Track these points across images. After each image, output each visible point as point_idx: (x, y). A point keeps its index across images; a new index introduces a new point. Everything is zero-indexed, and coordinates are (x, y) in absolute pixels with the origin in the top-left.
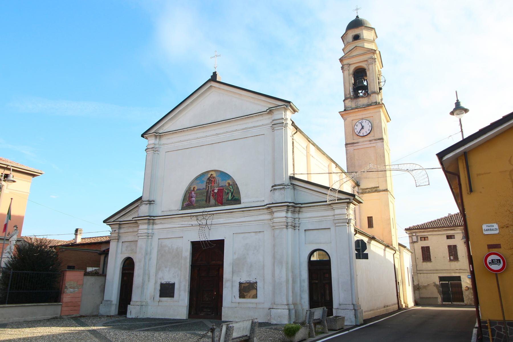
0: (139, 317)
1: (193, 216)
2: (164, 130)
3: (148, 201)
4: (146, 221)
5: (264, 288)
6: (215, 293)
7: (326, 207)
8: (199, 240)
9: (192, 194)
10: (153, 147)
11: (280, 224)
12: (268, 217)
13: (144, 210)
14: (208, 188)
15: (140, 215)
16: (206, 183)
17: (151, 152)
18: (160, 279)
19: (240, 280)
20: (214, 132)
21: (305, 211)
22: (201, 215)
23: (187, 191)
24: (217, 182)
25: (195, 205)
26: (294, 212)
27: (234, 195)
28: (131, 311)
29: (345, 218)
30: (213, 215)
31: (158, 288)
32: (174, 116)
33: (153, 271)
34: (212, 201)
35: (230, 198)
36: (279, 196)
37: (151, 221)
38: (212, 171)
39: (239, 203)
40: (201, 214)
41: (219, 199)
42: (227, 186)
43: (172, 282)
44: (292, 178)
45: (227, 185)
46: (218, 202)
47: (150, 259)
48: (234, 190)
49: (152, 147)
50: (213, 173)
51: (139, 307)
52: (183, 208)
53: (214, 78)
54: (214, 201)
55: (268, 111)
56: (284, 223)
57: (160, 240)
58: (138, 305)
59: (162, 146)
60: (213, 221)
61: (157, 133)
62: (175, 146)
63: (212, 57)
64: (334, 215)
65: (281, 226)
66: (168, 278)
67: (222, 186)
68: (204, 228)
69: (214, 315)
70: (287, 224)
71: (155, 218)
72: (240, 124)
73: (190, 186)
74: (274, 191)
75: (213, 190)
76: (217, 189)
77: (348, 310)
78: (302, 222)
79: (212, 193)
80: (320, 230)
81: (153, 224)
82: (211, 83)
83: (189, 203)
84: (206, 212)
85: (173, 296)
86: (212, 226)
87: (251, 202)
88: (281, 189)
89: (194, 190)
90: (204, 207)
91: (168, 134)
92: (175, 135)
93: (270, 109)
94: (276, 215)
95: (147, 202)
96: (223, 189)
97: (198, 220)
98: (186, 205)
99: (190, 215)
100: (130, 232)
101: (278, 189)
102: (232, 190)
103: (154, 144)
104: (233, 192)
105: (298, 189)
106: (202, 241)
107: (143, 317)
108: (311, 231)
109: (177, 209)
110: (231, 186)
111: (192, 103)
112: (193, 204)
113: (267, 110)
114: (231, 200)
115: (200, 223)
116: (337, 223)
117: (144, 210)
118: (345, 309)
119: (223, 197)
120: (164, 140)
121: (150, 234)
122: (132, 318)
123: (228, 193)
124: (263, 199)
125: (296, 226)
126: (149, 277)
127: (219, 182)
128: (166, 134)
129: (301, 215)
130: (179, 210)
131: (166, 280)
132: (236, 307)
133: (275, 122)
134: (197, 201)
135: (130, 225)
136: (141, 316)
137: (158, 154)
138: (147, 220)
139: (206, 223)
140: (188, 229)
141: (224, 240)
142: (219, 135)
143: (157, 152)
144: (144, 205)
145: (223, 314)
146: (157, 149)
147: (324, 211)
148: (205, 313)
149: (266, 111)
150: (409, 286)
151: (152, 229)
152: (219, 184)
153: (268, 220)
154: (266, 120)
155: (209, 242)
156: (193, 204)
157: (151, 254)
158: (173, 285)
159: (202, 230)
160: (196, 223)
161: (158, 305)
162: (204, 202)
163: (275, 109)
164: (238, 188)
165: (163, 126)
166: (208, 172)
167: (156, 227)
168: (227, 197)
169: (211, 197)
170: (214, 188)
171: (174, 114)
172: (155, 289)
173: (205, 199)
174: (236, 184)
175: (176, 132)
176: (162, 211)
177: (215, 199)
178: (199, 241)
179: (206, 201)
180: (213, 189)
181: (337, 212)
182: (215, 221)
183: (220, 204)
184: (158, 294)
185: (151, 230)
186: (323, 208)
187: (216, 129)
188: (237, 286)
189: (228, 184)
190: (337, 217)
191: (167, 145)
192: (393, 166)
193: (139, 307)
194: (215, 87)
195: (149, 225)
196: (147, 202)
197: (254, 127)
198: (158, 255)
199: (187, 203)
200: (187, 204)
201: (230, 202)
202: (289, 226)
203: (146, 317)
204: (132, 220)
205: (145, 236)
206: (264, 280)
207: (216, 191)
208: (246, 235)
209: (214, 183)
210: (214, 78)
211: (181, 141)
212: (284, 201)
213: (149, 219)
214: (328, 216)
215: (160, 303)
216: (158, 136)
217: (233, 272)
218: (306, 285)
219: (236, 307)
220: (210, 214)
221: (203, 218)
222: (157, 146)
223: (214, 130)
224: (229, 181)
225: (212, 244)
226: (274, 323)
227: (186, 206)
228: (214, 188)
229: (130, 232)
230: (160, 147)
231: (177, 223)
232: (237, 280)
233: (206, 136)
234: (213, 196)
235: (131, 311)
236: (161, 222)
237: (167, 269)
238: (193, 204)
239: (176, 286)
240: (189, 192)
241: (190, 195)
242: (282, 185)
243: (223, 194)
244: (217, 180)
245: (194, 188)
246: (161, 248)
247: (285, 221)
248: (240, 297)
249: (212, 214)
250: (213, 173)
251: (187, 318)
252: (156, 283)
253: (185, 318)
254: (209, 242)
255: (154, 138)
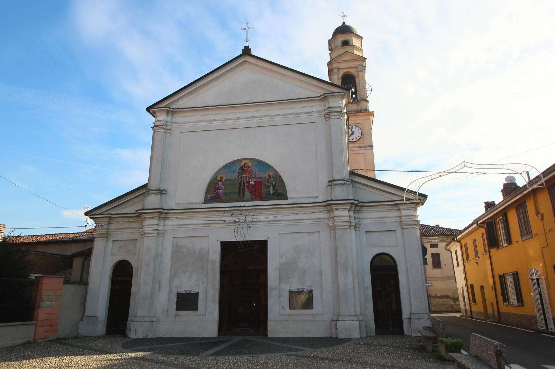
0: (149, 337)
1: (227, 211)
2: (179, 106)
3: (159, 190)
4: (157, 215)
5: (322, 297)
6: (255, 304)
7: (390, 207)
8: (236, 240)
9: (219, 184)
10: (165, 124)
11: (343, 223)
12: (324, 215)
13: (153, 201)
14: (240, 179)
15: (147, 207)
16: (239, 173)
17: (160, 131)
18: (177, 287)
19: (290, 288)
20: (289, 112)
21: (365, 211)
22: (237, 210)
23: (211, 181)
24: (254, 172)
25: (224, 198)
26: (354, 212)
27: (276, 189)
28: (136, 330)
29: (414, 220)
30: (255, 210)
31: (175, 299)
32: (194, 90)
33: (165, 277)
34: (248, 194)
35: (271, 192)
36: (339, 193)
37: (163, 215)
38: (246, 159)
39: (286, 198)
40: (238, 208)
41: (257, 193)
42: (267, 177)
43: (194, 290)
44: (352, 173)
45: (267, 177)
46: (255, 195)
47: (161, 263)
48: (276, 183)
49: (163, 124)
50: (247, 162)
51: (150, 323)
52: (206, 202)
53: (247, 51)
54: (250, 194)
55: (322, 97)
56: (348, 223)
57: (174, 239)
58: (148, 322)
59: (175, 125)
60: (254, 217)
61: (170, 108)
62: (194, 126)
63: (243, 29)
64: (400, 217)
65: (344, 226)
66: (187, 286)
67: (261, 178)
68: (241, 226)
69: (253, 330)
70: (350, 224)
71: (170, 211)
72: (283, 109)
73: (216, 175)
74: (334, 186)
75: (249, 182)
76: (254, 180)
77: (423, 320)
78: (363, 222)
79: (247, 186)
80: (383, 233)
81: (166, 218)
82: (245, 58)
83: (214, 195)
84: (244, 206)
85: (196, 309)
86: (253, 223)
87: (301, 198)
88: (342, 184)
89: (221, 180)
90: (238, 201)
91: (185, 110)
92: (194, 114)
93: (325, 95)
94: (336, 213)
95: (157, 192)
96: (262, 181)
97: (233, 216)
98: (210, 197)
99: (222, 209)
100: (126, 228)
101: (338, 184)
102: (274, 183)
103: (166, 122)
104: (276, 185)
105: (356, 186)
106: (238, 241)
107: (153, 337)
108: (373, 233)
109: (199, 201)
110: (273, 178)
111: (218, 77)
112: (221, 196)
113: (320, 95)
114: (274, 194)
115: (235, 219)
116: (404, 225)
117: (153, 201)
118: (420, 319)
119: (263, 191)
120: (178, 118)
121: (163, 231)
122: (138, 339)
123: (268, 186)
124: (316, 195)
125: (356, 226)
126: (160, 285)
127: (255, 173)
128: (182, 111)
129: (361, 215)
130: (202, 204)
131: (185, 289)
132: (286, 320)
133: (330, 110)
134: (226, 194)
135: (129, 219)
136: (151, 336)
137: (170, 134)
138: (159, 213)
139: (245, 220)
140: (216, 227)
141: (267, 240)
142: (256, 119)
143: (169, 131)
144: (153, 195)
145: (269, 329)
146: (169, 128)
147: (385, 211)
148: (241, 328)
149: (320, 97)
150: (493, 290)
151: (164, 225)
152: (256, 175)
153: (324, 219)
154: (317, 107)
155: (249, 242)
156: (221, 196)
157: (162, 257)
158: (196, 295)
159: (239, 228)
160: (230, 219)
161: (175, 321)
162: (237, 196)
163: (331, 96)
164: (282, 181)
165: (177, 101)
166: (240, 160)
167: (168, 222)
168: (267, 191)
169: (246, 190)
170: (249, 179)
171: (194, 88)
172: (169, 300)
173: (238, 192)
174: (280, 177)
175: (196, 110)
176: (177, 203)
177: (251, 193)
178: (236, 241)
179: (239, 194)
180: (248, 180)
181: (404, 213)
182: (256, 218)
183: (258, 199)
184: (174, 306)
185: (162, 227)
186: (387, 208)
187: (251, 112)
188: (287, 294)
189: (268, 176)
190: (404, 219)
191: (183, 123)
192: (496, 165)
193: (150, 323)
194: (250, 63)
195: (159, 220)
196: (157, 192)
197: (278, 115)
198: (172, 258)
199: (212, 195)
200: (212, 197)
201: (271, 196)
202: (352, 226)
203: (156, 336)
204: (135, 213)
205: (154, 234)
206: (321, 288)
207: (252, 183)
208: (297, 235)
209: (250, 174)
210: (247, 51)
211: (202, 121)
212: (347, 199)
213: (161, 213)
214: (394, 217)
215: (177, 318)
216: (171, 112)
217: (281, 279)
218: (370, 292)
219: (286, 320)
220: (250, 210)
221: (240, 214)
222: (169, 124)
223: (249, 112)
224: (270, 173)
225: (253, 245)
226: (341, 338)
227: (211, 199)
228: (249, 179)
229: (126, 228)
230: (173, 125)
231: (201, 219)
232: (286, 288)
233: (238, 118)
234: (248, 188)
235: (136, 330)
236: (176, 217)
237: (187, 275)
238: (221, 197)
239: (201, 297)
240: (215, 182)
241: (216, 186)
242: (343, 181)
243: (261, 186)
244: (253, 170)
245: (221, 178)
246: (177, 251)
247: (348, 220)
248: (290, 308)
249: (254, 210)
250: (247, 162)
251: (218, 336)
252: (170, 292)
253: (216, 337)
254: (249, 242)
255: (165, 114)
